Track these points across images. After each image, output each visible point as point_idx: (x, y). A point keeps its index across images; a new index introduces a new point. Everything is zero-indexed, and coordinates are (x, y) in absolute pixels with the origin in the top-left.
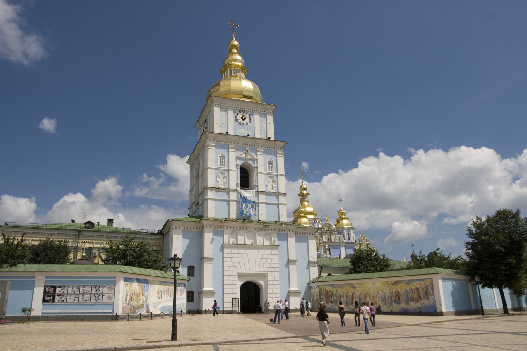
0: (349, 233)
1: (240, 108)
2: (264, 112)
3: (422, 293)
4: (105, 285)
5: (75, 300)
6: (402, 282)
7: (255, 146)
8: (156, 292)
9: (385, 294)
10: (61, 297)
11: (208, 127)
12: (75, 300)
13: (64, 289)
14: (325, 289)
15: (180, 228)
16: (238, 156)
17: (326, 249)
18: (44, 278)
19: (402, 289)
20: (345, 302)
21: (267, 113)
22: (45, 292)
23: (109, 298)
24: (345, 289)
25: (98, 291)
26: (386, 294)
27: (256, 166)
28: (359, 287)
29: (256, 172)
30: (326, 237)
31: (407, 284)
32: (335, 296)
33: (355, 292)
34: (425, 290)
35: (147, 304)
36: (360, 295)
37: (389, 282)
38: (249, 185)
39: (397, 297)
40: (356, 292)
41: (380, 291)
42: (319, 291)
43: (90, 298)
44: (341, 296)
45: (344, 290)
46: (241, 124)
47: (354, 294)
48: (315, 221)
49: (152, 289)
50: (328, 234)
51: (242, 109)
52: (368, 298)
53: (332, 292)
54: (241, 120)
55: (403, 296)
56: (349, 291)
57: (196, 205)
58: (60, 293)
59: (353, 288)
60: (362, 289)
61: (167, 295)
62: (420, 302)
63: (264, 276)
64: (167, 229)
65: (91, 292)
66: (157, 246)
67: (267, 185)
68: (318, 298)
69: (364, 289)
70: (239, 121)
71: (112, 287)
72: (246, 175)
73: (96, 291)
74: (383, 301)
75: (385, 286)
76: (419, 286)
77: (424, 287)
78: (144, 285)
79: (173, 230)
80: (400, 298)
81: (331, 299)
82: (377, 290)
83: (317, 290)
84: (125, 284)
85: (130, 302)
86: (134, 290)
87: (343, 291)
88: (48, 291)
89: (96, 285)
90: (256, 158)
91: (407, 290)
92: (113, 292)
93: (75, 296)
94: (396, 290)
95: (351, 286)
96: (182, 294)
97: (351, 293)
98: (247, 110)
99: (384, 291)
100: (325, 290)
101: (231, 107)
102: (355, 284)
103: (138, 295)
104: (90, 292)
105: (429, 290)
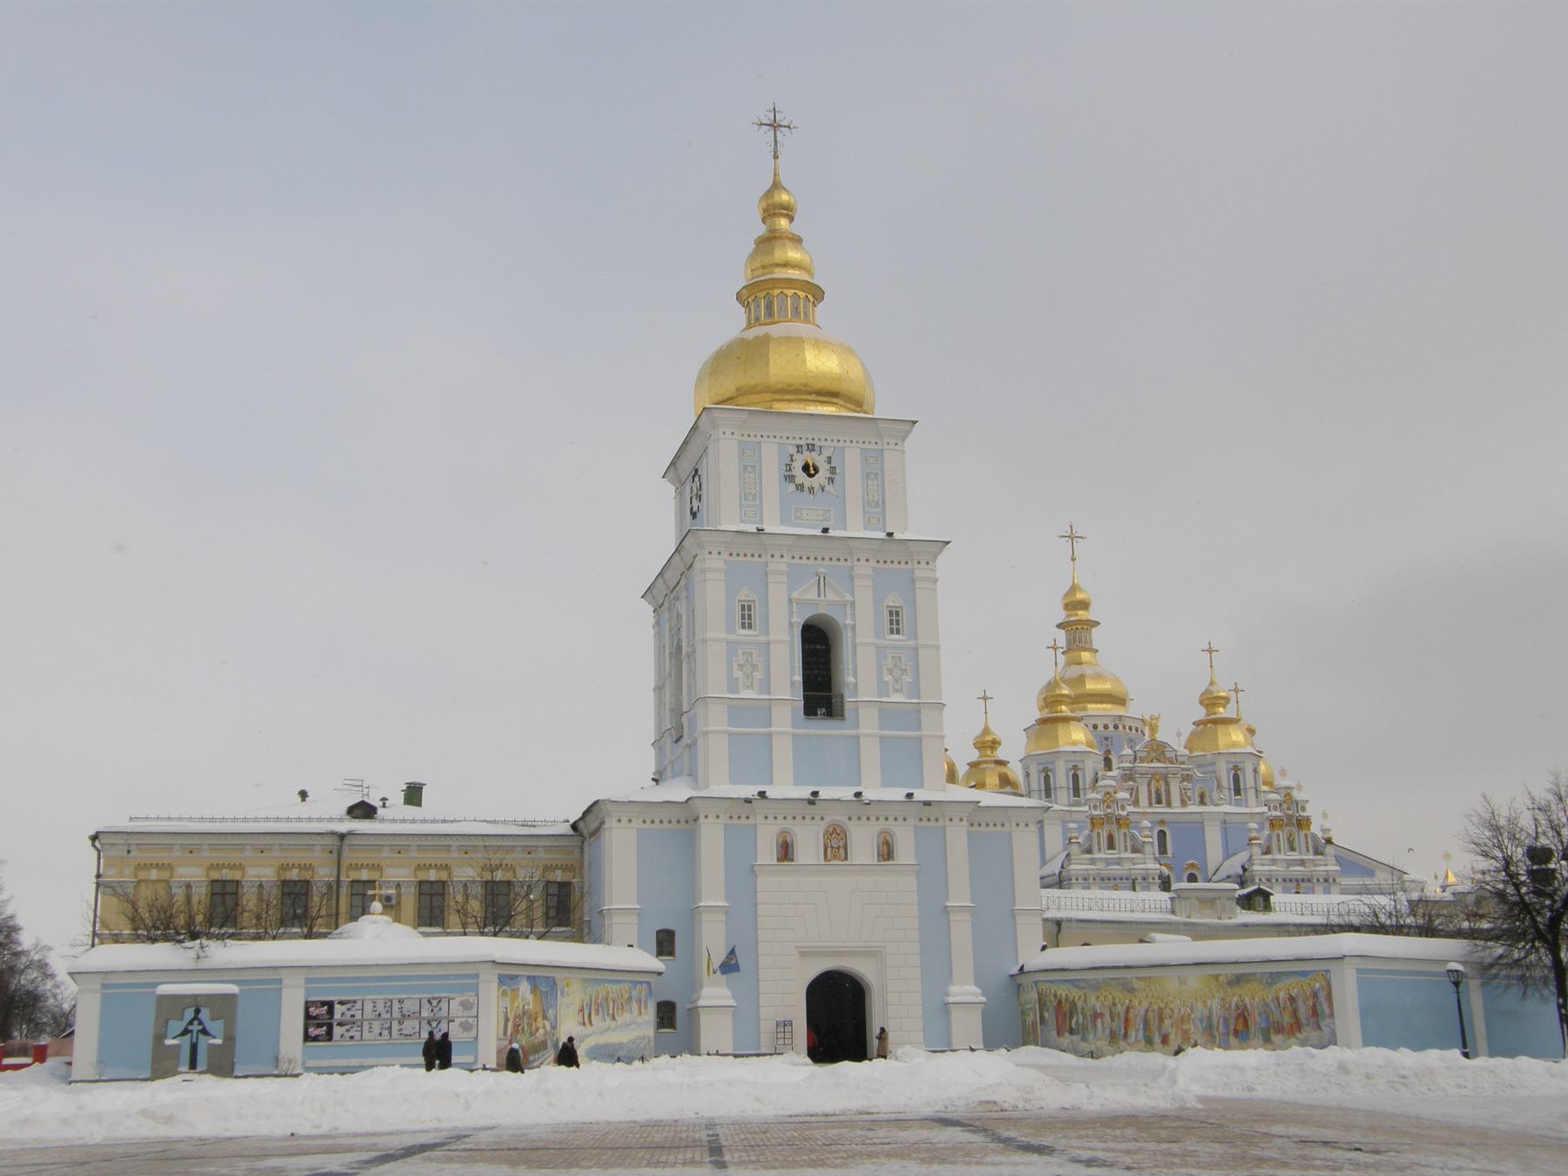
0: (1239, 772)
1: (801, 438)
2: (876, 443)
3: (1303, 1011)
4: (452, 996)
5: (381, 1034)
7: (846, 560)
8: (577, 1007)
9: (1210, 1012)
10: (348, 1027)
11: (704, 498)
12: (381, 1034)
13: (353, 1009)
14: (1055, 991)
16: (795, 595)
18: (302, 981)
19: (1253, 999)
20: (1107, 1031)
21: (886, 447)
22: (308, 1016)
23: (466, 1027)
25: (435, 1010)
26: (1214, 1012)
27: (849, 624)
28: (1144, 990)
30: (1149, 791)
31: (1267, 982)
32: (1082, 1013)
33: (1133, 1003)
34: (1311, 1004)
35: (555, 1042)
36: (1147, 1011)
39: (1241, 1021)
40: (1137, 1004)
42: (1040, 999)
43: (417, 1030)
44: (1096, 1015)
45: (1105, 996)
46: (802, 490)
47: (1131, 1010)
48: (1116, 727)
49: (564, 1000)
50: (1157, 781)
52: (1167, 1022)
53: (1073, 1001)
54: (801, 477)
55: (1257, 1016)
56: (1117, 1001)
57: (677, 741)
58: (344, 1018)
59: (1129, 991)
60: (1153, 996)
61: (603, 1012)
62: (1298, 1034)
63: (874, 953)
64: (592, 823)
65: (420, 1014)
66: (565, 868)
67: (888, 678)
68: (1036, 1020)
70: (798, 481)
71: (471, 1000)
73: (432, 1011)
74: (1205, 1030)
75: (1210, 989)
76: (1296, 991)
77: (1308, 993)
78: (547, 992)
79: (611, 828)
80: (1250, 1023)
81: (1070, 1023)
83: (1034, 995)
84: (501, 991)
85: (514, 1036)
86: (524, 1007)
88: (314, 1015)
89: (430, 996)
90: (849, 597)
91: (1267, 1001)
92: (474, 1012)
93: (383, 1025)
95: (1123, 985)
96: (643, 1011)
97: (1122, 1005)
98: (822, 443)
99: (1209, 1002)
100: (1055, 996)
101: (771, 439)
102: (1134, 980)
103: (534, 1016)
104: (418, 1014)
105: (1321, 1006)
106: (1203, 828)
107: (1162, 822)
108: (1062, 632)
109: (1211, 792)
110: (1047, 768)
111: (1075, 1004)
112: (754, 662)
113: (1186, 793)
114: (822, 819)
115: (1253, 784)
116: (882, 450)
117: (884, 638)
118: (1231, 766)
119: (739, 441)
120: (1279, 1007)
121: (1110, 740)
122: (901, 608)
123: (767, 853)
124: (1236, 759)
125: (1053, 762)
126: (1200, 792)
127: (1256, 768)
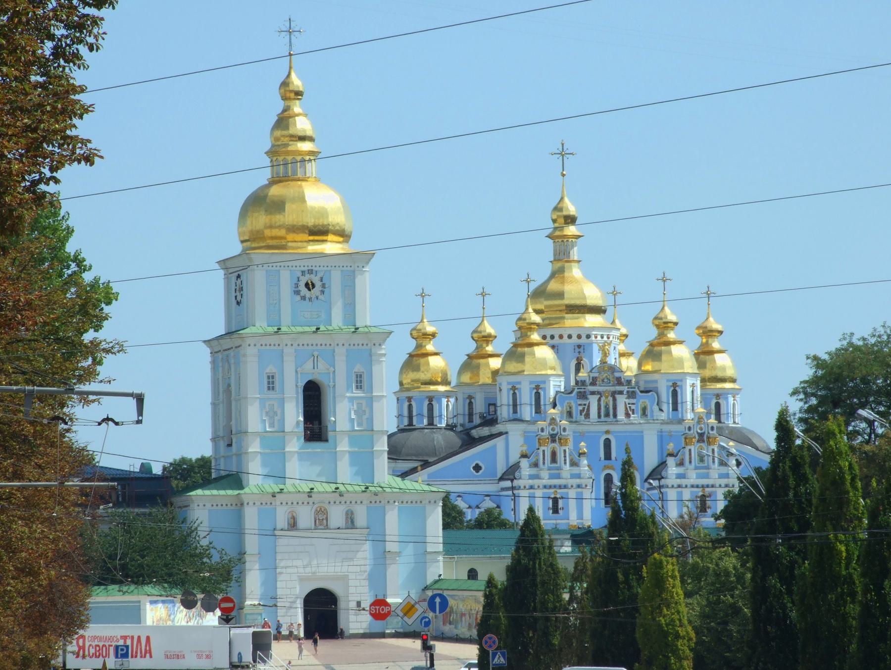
0: (677, 388)
2: (351, 267)
11: (244, 296)
15: (204, 505)
17: (580, 455)
29: (332, 395)
38: (322, 411)
44: (463, 615)
50: (607, 397)
51: (308, 266)
54: (304, 291)
70: (302, 294)
72: (317, 393)
87: (465, 606)
98: (317, 269)
101: (286, 268)
106: (642, 437)
107: (607, 432)
111: (453, 609)
112: (275, 410)
113: (630, 407)
114: (314, 503)
116: (354, 271)
117: (353, 393)
118: (671, 384)
119: (266, 271)
121: (582, 347)
122: (363, 372)
123: (282, 521)
124: (674, 378)
125: (519, 383)
126: (643, 406)
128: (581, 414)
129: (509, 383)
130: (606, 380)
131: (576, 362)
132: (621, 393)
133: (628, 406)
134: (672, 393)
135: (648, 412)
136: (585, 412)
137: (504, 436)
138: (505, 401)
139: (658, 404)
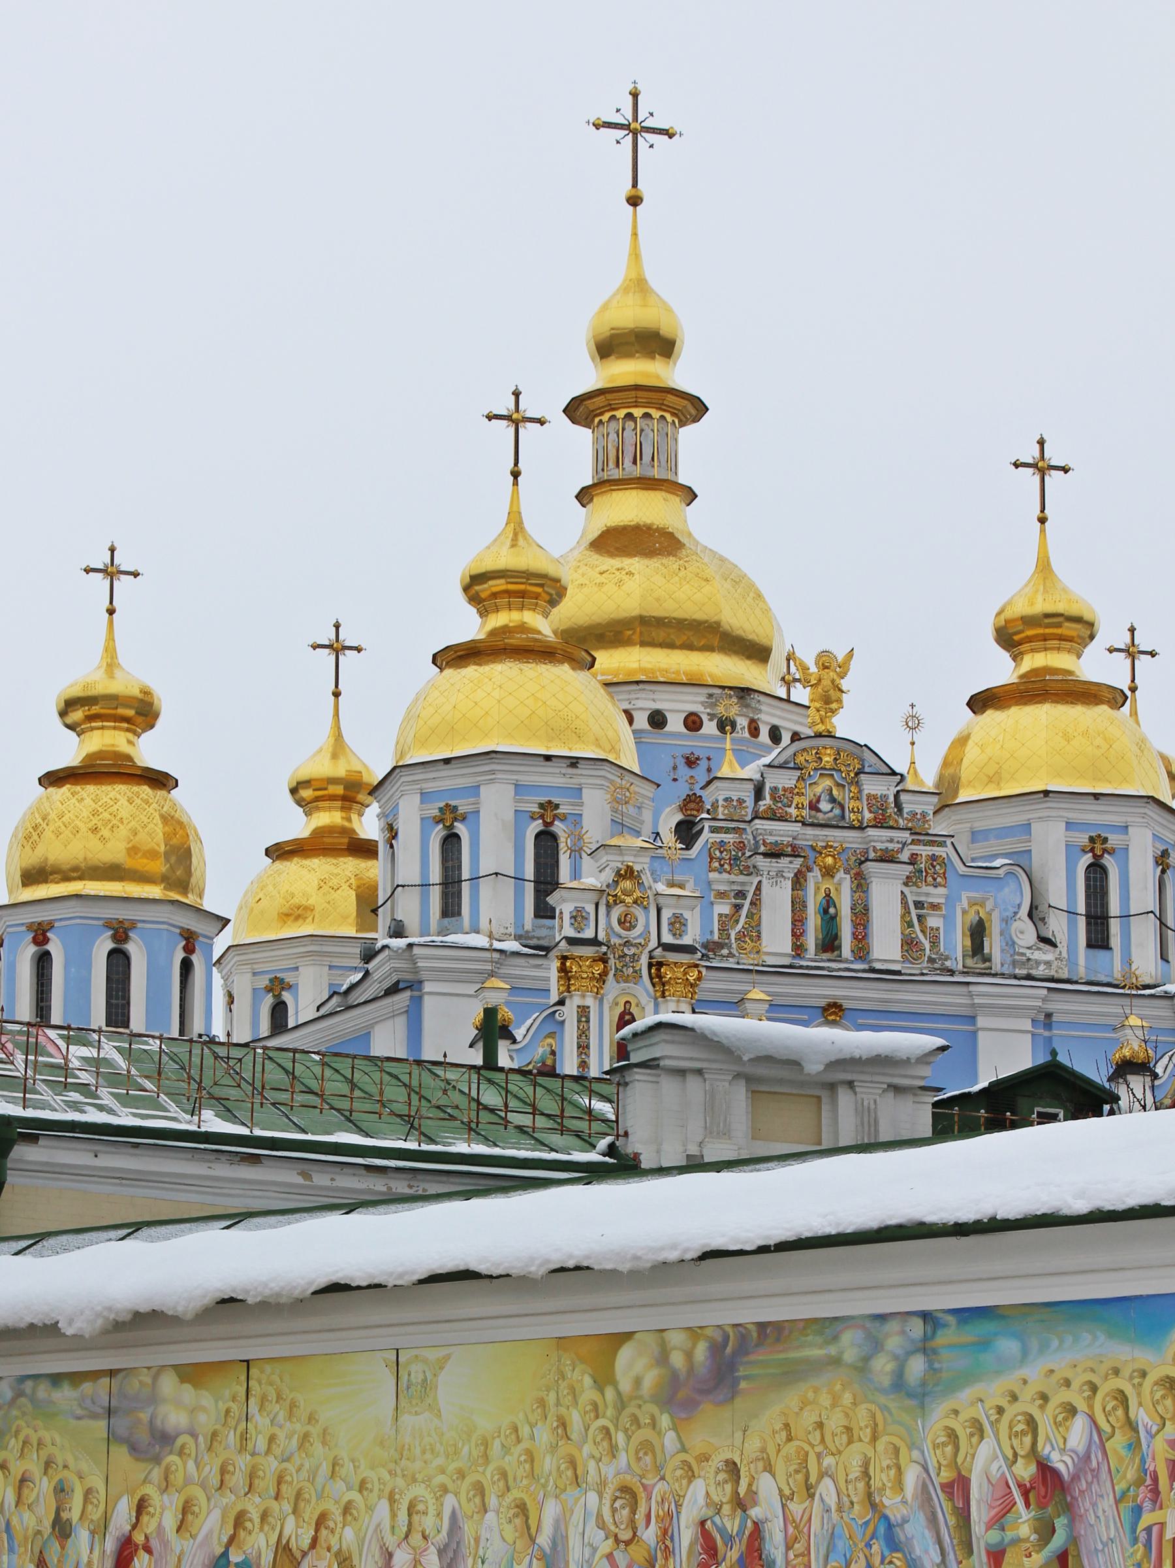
0: (1108, 861)
6: (816, 1352)
19: (810, 1491)
24: (33, 1465)
30: (798, 908)
31: (899, 1384)
33: (149, 1525)
37: (625, 1354)
40: (170, 1521)
41: (491, 1516)
45: (23, 1480)
48: (725, 725)
50: (828, 872)
59: (134, 1449)
60: (252, 1476)
69: (280, 1481)
75: (563, 1424)
76: (1078, 1433)
82: (445, 1490)
91: (890, 1502)
94: (723, 1494)
97: (101, 1529)
99: (551, 1510)
102: (168, 1384)
106: (974, 1034)
108: (584, 435)
109: (1006, 921)
110: (456, 808)
115: (1152, 904)
118: (1083, 839)
120: (969, 1549)
121: (703, 764)
125: (475, 790)
126: (972, 917)
127: (1165, 854)
128: (723, 930)
129: (425, 796)
130: (825, 806)
131: (679, 817)
132: (887, 858)
133: (914, 912)
134: (1087, 879)
135: (994, 945)
136: (739, 927)
137: (408, 994)
138: (409, 871)
139: (1030, 915)
